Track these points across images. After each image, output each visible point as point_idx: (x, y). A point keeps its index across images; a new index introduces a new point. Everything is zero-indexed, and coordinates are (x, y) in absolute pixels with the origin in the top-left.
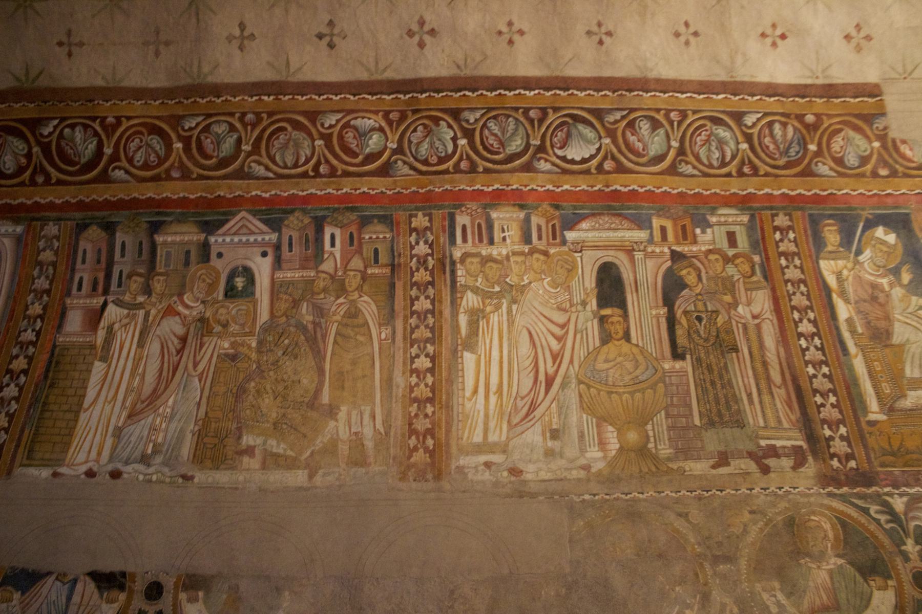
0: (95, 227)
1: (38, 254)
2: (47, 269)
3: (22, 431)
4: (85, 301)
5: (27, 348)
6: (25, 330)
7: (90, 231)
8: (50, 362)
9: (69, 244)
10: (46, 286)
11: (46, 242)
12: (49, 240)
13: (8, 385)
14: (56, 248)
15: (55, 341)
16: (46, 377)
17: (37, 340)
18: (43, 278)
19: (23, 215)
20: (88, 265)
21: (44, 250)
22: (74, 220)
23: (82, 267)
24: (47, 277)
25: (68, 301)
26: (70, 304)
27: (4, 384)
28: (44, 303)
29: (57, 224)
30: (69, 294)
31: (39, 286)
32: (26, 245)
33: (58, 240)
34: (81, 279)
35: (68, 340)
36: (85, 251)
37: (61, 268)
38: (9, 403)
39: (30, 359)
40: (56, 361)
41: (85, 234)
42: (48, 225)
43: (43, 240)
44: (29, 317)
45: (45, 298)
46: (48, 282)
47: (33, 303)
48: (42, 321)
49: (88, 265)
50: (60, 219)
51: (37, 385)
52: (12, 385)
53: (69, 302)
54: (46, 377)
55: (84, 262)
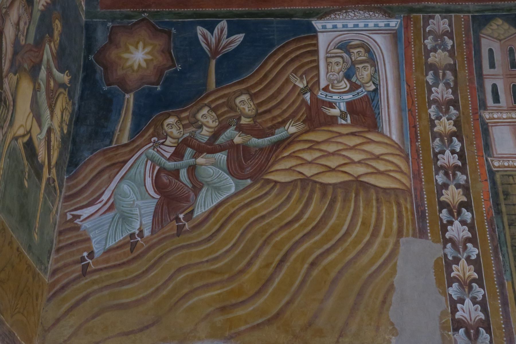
0: (500, 22)
1: (428, 57)
2: (444, 74)
3: (502, 285)
4: (509, 115)
5: (454, 175)
6: (443, 152)
7: (495, 27)
8: (495, 195)
9: (468, 43)
10: (449, 95)
11: (435, 39)
12: (439, 37)
13: (451, 223)
14: (449, 48)
15: (489, 166)
16: (499, 212)
17: (464, 164)
18: (441, 86)
19: (395, 5)
20: (498, 70)
21: (434, 50)
22: (469, 12)
23: (492, 71)
24: (447, 85)
25: (486, 115)
26: (490, 119)
27: (445, 222)
28: (454, 118)
29: (445, 17)
30: (484, 106)
31: (440, 96)
32: (408, 43)
33: (451, 38)
34: (495, 88)
35: (506, 164)
36: (491, 51)
37: (464, 74)
38: (465, 248)
39: (466, 189)
40: (503, 192)
41: (487, 30)
42: (433, 18)
43: (430, 37)
44: (440, 135)
45: (453, 110)
46: (450, 90)
47: (439, 118)
48: (461, 140)
49: (498, 70)
50: (448, 11)
51: (491, 224)
52: (457, 223)
53: (487, 116)
54: (499, 212)
55: (492, 65)
